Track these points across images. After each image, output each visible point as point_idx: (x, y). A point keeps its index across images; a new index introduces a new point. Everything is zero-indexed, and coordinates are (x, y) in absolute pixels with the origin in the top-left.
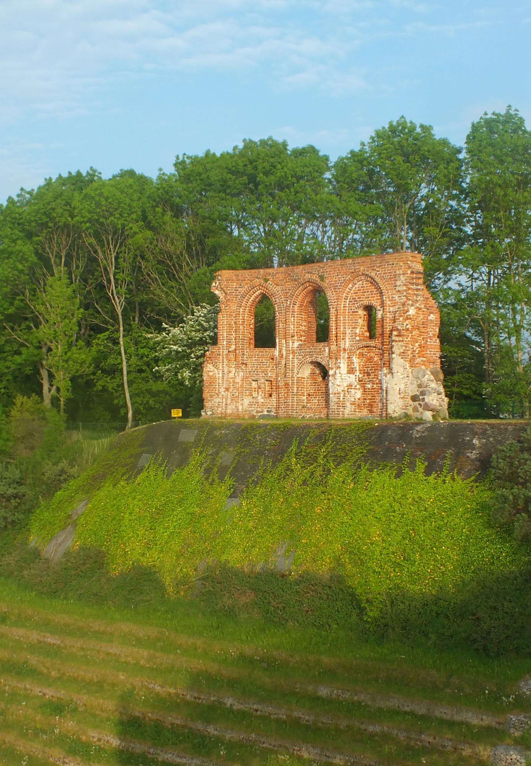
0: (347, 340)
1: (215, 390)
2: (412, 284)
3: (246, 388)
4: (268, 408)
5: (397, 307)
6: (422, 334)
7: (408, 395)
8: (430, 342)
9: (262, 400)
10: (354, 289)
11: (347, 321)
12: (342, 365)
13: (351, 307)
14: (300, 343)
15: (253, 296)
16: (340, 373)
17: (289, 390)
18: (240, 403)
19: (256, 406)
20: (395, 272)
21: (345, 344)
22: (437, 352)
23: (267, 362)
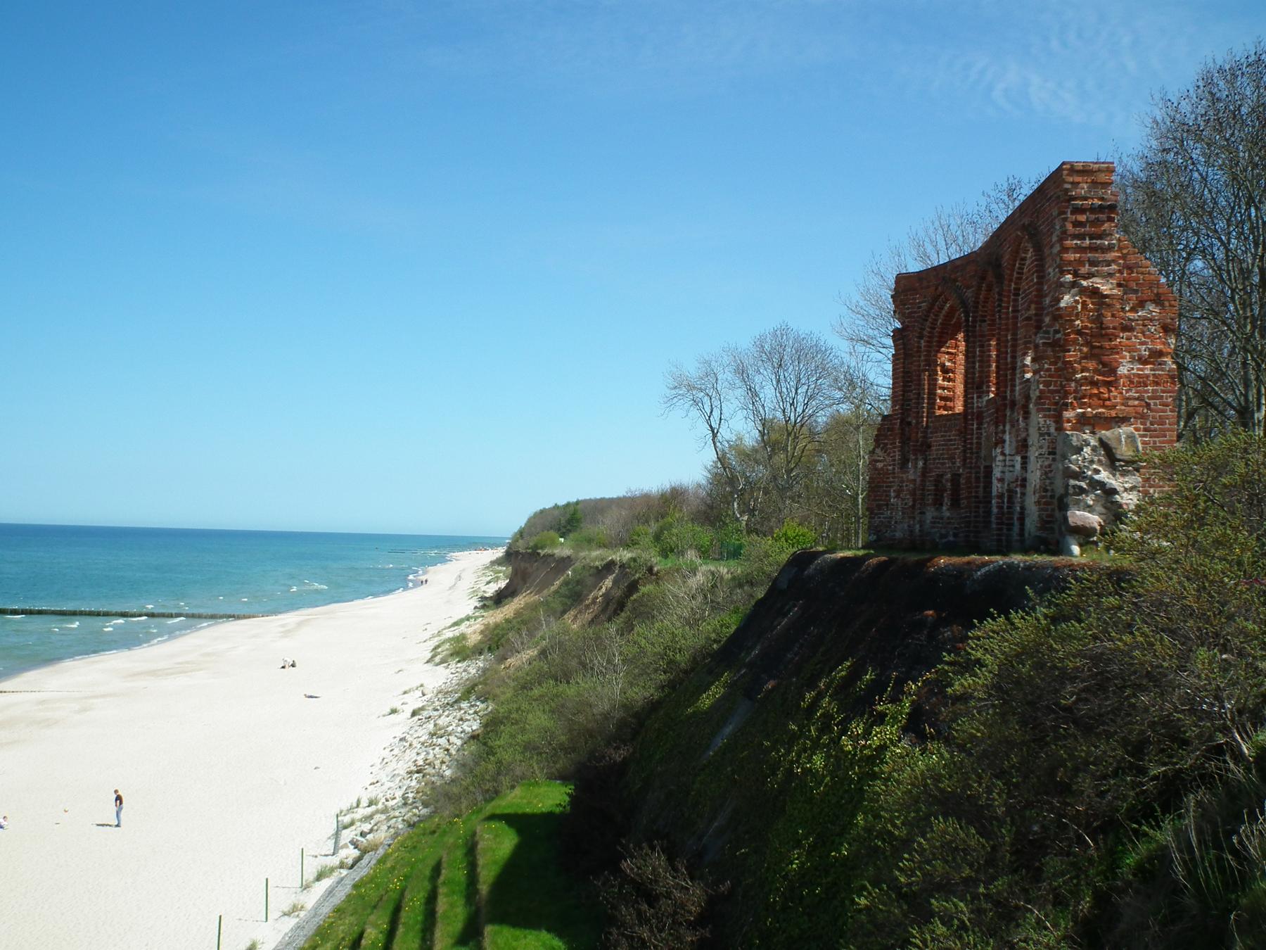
0: (1018, 381)
1: (887, 496)
2: (1081, 237)
3: (928, 490)
4: (956, 528)
5: (1051, 295)
6: (1096, 351)
7: (1052, 497)
8: (1138, 369)
9: (948, 514)
10: (1025, 270)
11: (1019, 342)
12: (1007, 437)
13: (1022, 310)
14: (992, 395)
15: (942, 316)
16: (1003, 454)
17: (971, 492)
18: (918, 519)
19: (940, 525)
20: (1052, 215)
21: (1013, 391)
22: (1163, 392)
23: (955, 440)
